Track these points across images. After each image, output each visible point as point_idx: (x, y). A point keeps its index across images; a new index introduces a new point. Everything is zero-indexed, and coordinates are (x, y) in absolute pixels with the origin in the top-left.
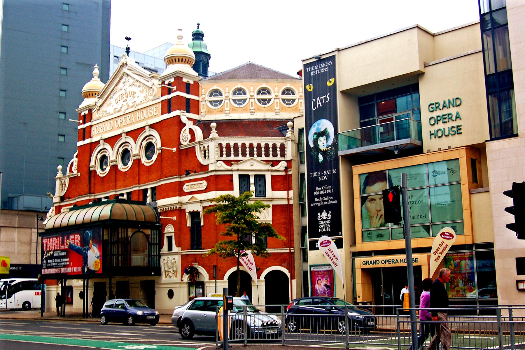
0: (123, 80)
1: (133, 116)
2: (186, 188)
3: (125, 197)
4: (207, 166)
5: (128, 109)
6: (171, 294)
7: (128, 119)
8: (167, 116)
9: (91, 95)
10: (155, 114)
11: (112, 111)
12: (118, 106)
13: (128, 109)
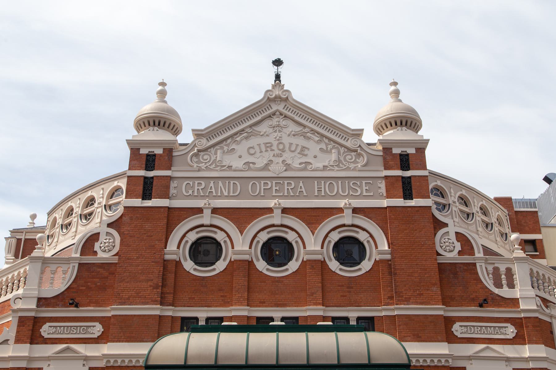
0: (275, 121)
1: (301, 184)
2: (457, 329)
5: (285, 171)
7: (286, 187)
8: (399, 202)
10: (365, 194)
11: (238, 164)
12: (260, 162)
13: (285, 171)
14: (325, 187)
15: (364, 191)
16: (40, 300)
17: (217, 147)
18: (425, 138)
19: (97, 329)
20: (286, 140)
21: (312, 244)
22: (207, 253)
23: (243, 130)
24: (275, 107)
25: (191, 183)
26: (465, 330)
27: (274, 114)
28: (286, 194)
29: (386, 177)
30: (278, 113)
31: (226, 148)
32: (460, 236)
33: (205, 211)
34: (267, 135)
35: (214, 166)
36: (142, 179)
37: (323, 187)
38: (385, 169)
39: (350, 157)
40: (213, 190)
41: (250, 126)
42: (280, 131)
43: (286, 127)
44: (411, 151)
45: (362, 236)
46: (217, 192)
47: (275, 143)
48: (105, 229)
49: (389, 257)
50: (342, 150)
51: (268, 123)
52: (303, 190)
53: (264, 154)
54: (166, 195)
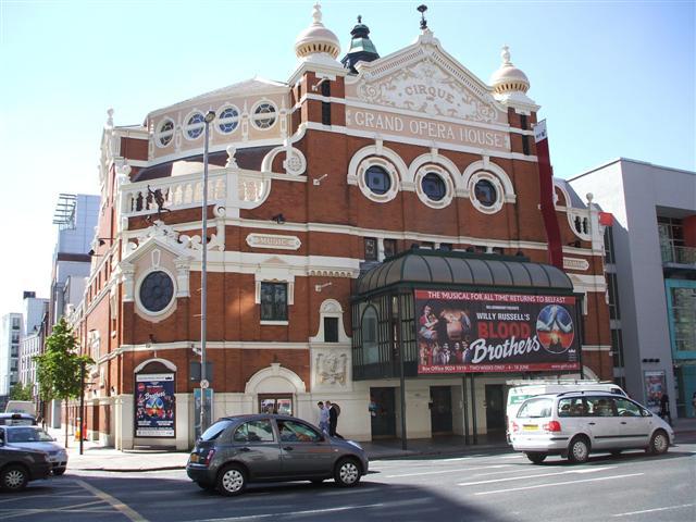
9: (317, 47)
11: (400, 102)
16: (242, 210)
18: (537, 104)
21: (461, 184)
22: (376, 181)
29: (511, 134)
33: (377, 142)
44: (528, 114)
45: (495, 182)
49: (514, 201)
54: (343, 123)
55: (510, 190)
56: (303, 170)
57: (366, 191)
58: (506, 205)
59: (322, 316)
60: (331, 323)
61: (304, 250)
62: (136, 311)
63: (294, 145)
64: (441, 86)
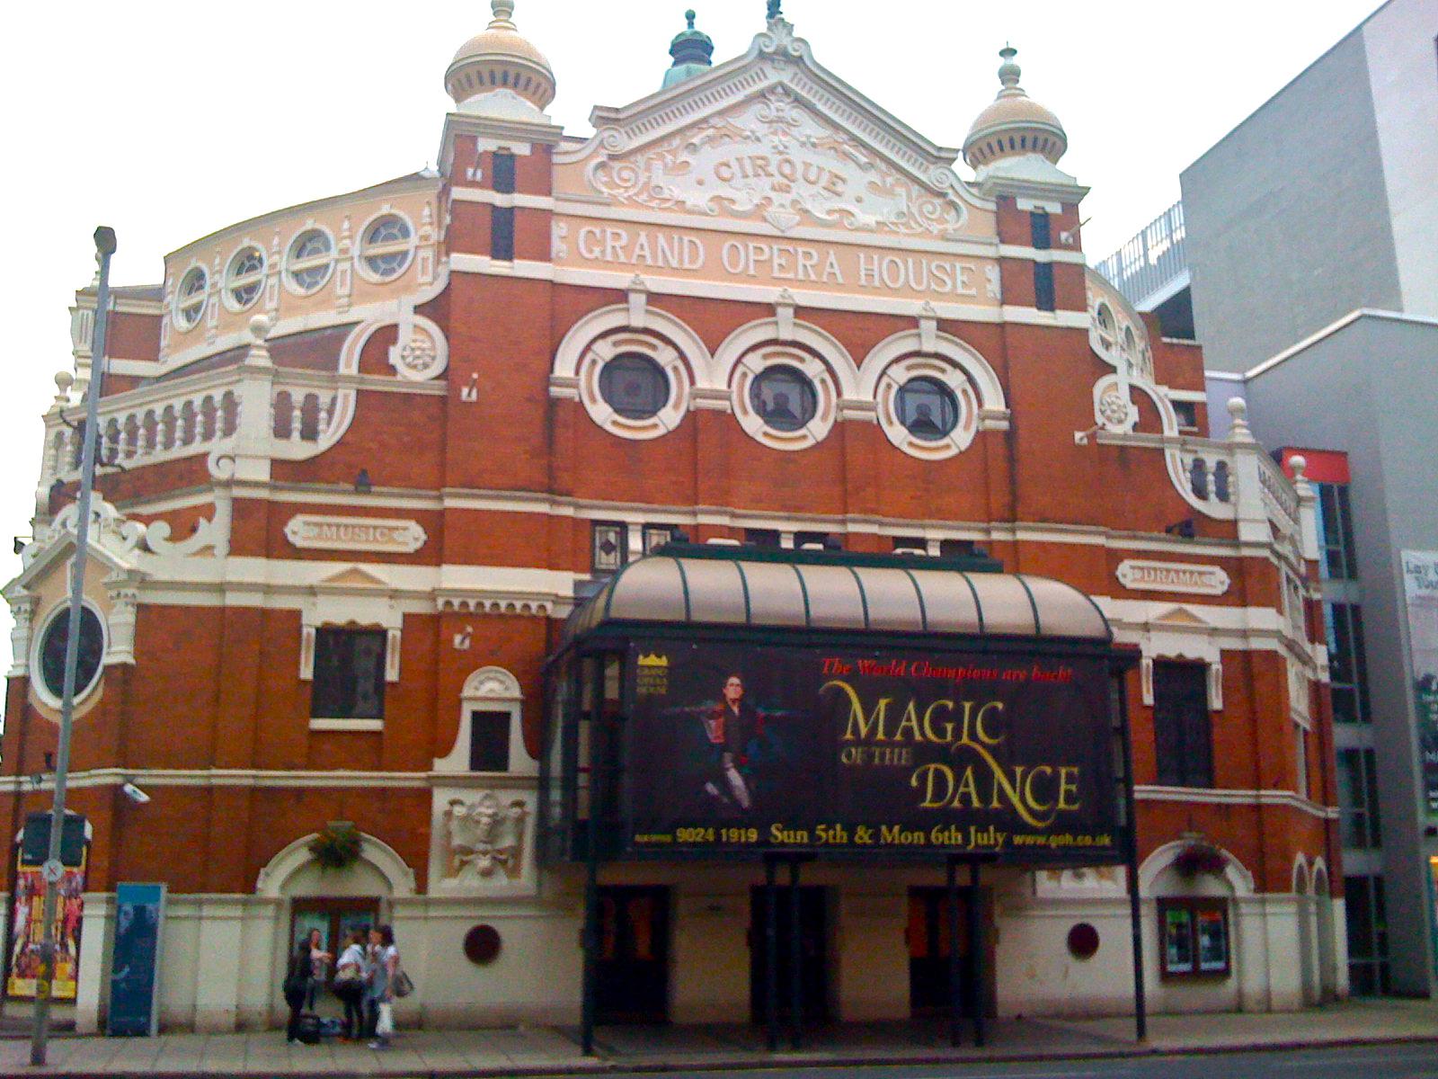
1: (832, 258)
3: (934, 552)
4: (1233, 524)
5: (798, 224)
6: (1083, 941)
7: (801, 261)
10: (960, 290)
11: (697, 198)
13: (798, 224)
14: (881, 264)
15: (959, 284)
17: (650, 154)
18: (1081, 183)
19: (412, 536)
20: (797, 155)
22: (633, 389)
23: (705, 120)
24: (773, 76)
25: (597, 231)
26: (1138, 574)
27: (772, 90)
28: (801, 276)
29: (1001, 261)
30: (780, 90)
31: (669, 158)
32: (1137, 394)
34: (758, 139)
35: (644, 197)
36: (489, 209)
37: (876, 267)
38: (1003, 241)
39: (930, 208)
40: (647, 253)
41: (721, 113)
42: (785, 133)
43: (793, 124)
44: (1054, 208)
45: (954, 380)
46: (655, 257)
47: (775, 159)
48: (408, 321)
49: (1004, 425)
50: (915, 189)
51: (758, 108)
52: (836, 270)
53: (752, 181)
54: (544, 255)
55: (994, 401)
56: (437, 368)
57: (601, 413)
58: (982, 436)
59: (467, 710)
60: (490, 729)
61: (431, 555)
62: (31, 700)
63: (418, 309)
64: (810, 156)
